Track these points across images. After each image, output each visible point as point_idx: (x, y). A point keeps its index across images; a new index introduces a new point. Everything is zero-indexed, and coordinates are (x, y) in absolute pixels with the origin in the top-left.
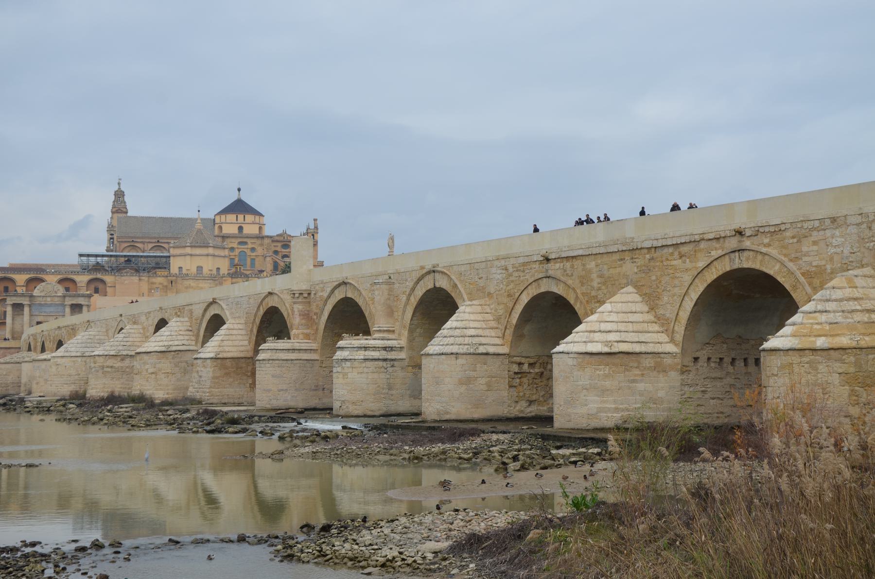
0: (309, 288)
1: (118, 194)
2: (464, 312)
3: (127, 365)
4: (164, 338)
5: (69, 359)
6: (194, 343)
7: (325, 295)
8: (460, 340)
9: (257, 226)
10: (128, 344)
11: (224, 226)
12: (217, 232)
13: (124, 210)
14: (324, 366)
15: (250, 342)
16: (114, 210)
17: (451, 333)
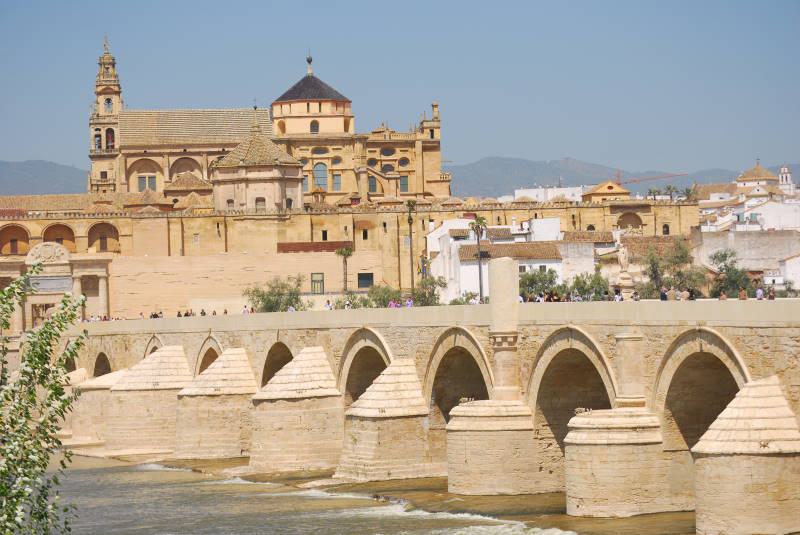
0: (515, 330)
1: (104, 64)
2: (748, 397)
3: (230, 408)
4: (293, 378)
5: (138, 393)
6: (334, 384)
7: (541, 341)
8: (744, 435)
9: (342, 120)
10: (230, 376)
11: (288, 122)
12: (276, 131)
13: (116, 89)
14: (539, 437)
15: (423, 394)
16: (100, 89)
17: (732, 424)
